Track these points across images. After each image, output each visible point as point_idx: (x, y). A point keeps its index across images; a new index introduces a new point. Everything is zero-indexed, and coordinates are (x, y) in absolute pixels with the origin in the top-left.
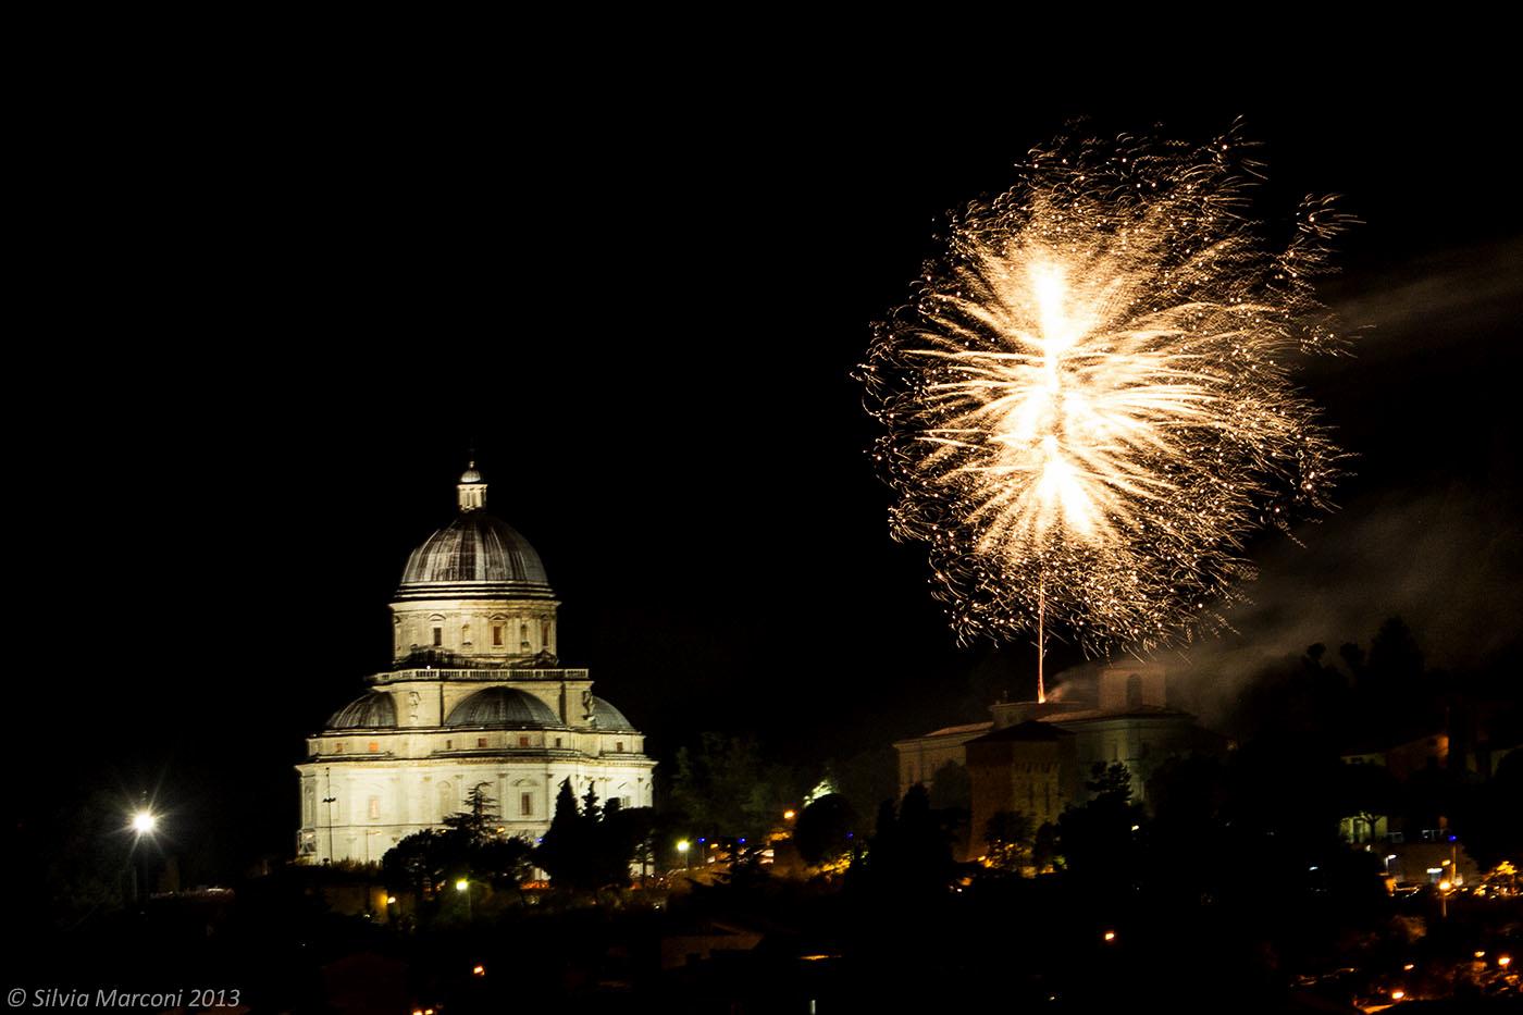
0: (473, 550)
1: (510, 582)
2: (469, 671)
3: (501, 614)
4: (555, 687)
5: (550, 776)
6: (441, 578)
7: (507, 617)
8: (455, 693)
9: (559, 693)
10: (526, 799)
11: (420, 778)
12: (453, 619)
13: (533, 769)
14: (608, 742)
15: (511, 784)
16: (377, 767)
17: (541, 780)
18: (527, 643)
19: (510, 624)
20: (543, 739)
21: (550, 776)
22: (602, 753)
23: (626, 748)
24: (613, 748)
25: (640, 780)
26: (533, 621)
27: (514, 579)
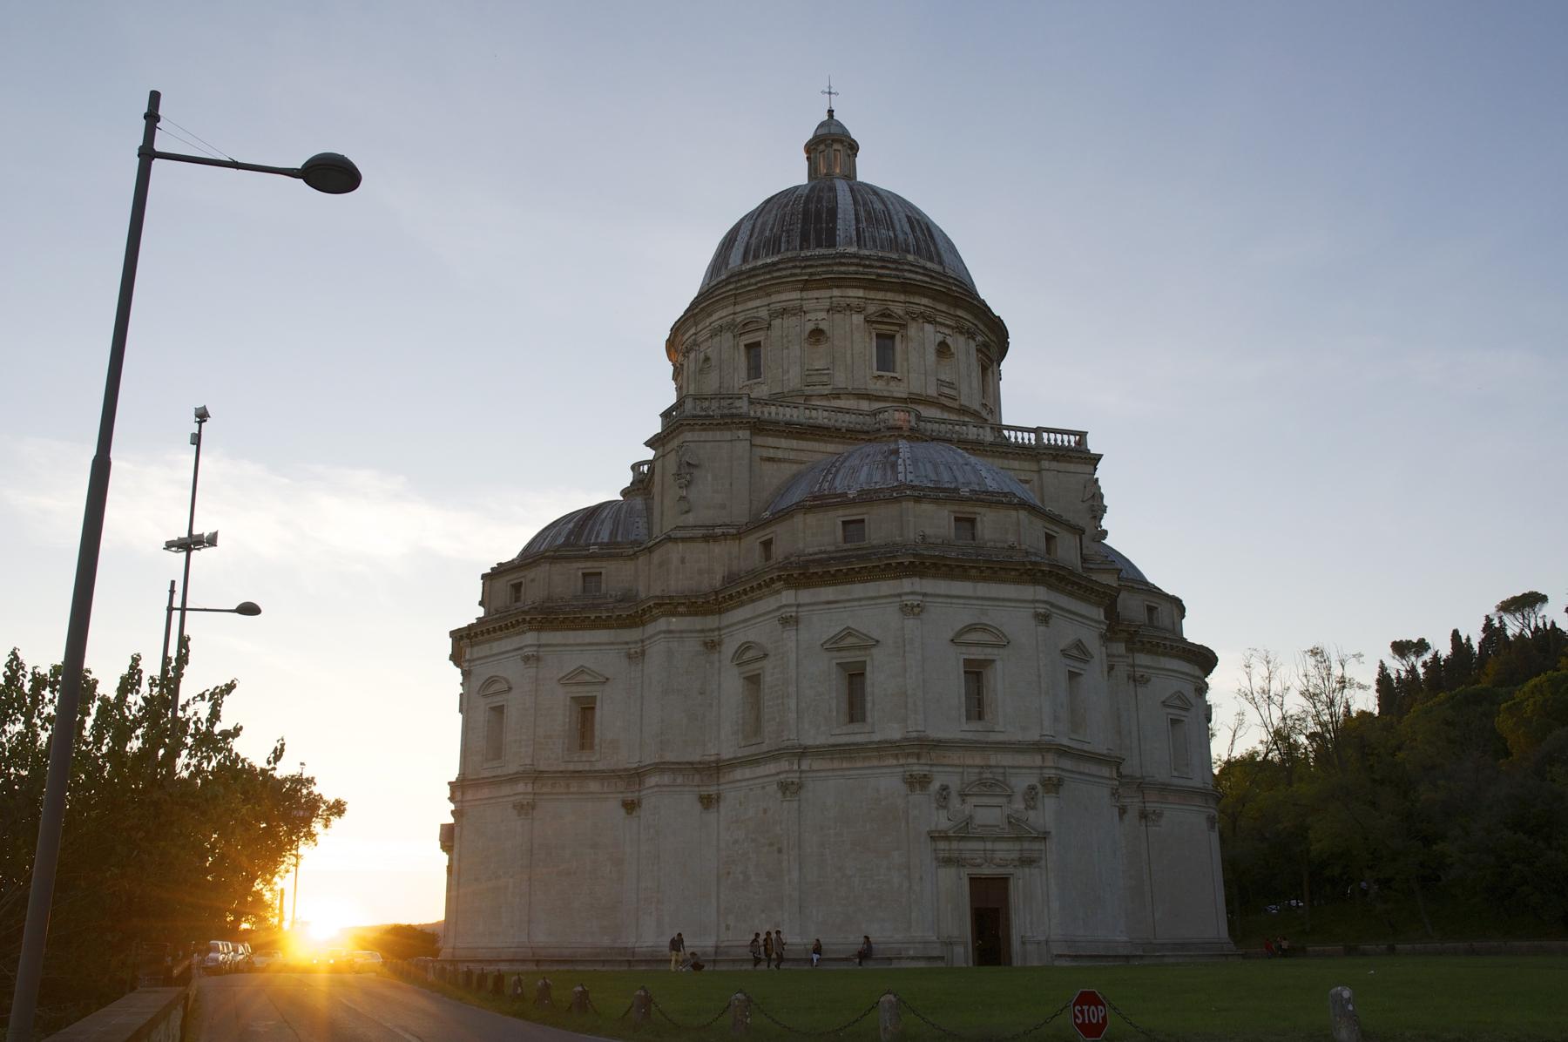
1: (910, 258)
6: (762, 252)
12: (790, 321)
19: (913, 330)
21: (1044, 619)
24: (1142, 617)
26: (961, 339)
27: (918, 252)
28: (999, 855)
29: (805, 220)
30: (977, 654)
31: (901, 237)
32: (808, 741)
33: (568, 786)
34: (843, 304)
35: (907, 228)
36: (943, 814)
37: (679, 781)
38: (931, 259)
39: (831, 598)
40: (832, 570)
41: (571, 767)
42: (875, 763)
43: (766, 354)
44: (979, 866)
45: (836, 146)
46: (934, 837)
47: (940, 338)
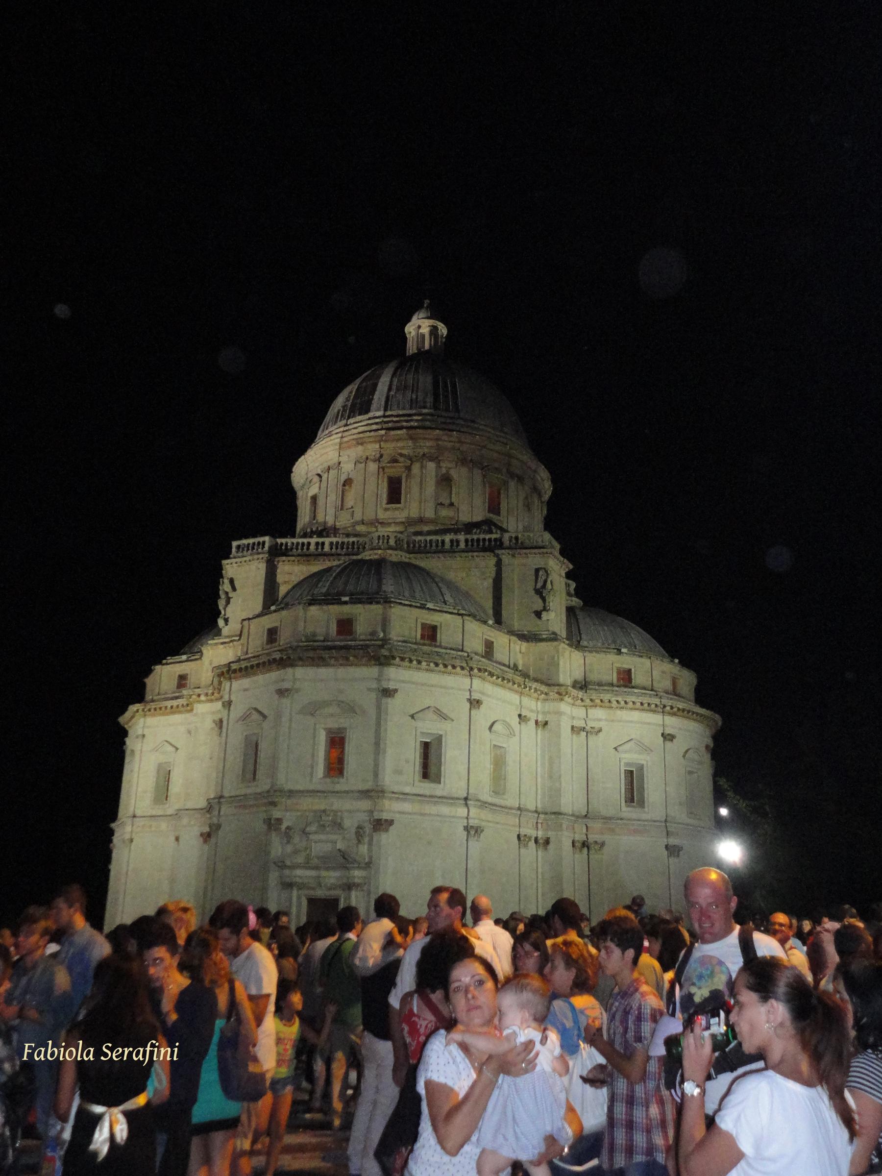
0: (379, 377)
1: (425, 411)
2: (327, 541)
3: (401, 455)
4: (483, 564)
5: (388, 693)
7: (411, 459)
8: (291, 573)
9: (492, 572)
10: (337, 741)
11: (209, 724)
13: (355, 680)
14: (605, 664)
15: (302, 712)
16: (173, 710)
17: (368, 701)
18: (452, 504)
19: (416, 469)
20: (385, 623)
22: (583, 685)
23: (638, 678)
25: (668, 737)
26: (464, 471)
27: (435, 408)
28: (332, 881)
29: (355, 397)
30: (333, 724)
31: (420, 398)
32: (226, 794)
33: (151, 826)
34: (364, 457)
35: (430, 387)
36: (289, 849)
37: (192, 823)
38: (447, 410)
39: (247, 686)
40: (243, 666)
41: (154, 813)
42: (255, 809)
43: (321, 502)
44: (313, 889)
45: (421, 331)
46: (281, 865)
47: (444, 471)
